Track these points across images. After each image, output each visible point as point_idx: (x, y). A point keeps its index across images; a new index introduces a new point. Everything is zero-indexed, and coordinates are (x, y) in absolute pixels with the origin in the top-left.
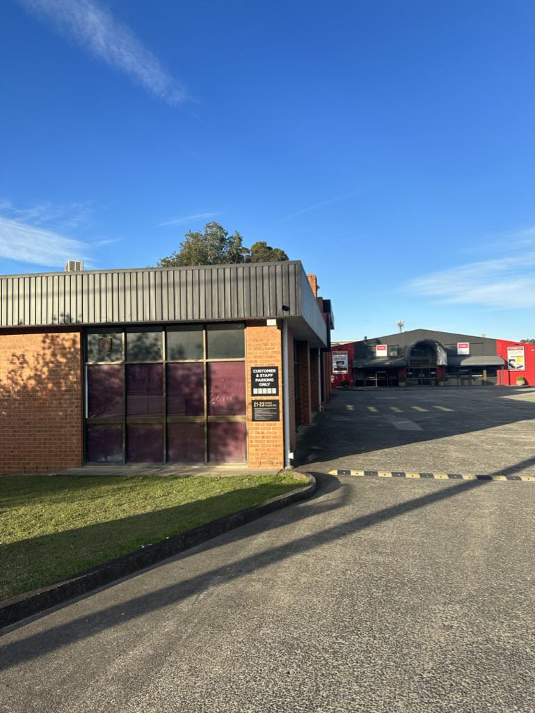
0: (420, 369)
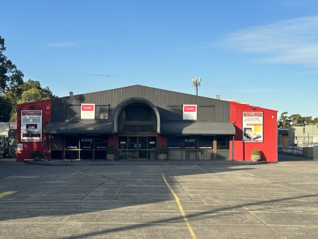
0: (136, 138)
